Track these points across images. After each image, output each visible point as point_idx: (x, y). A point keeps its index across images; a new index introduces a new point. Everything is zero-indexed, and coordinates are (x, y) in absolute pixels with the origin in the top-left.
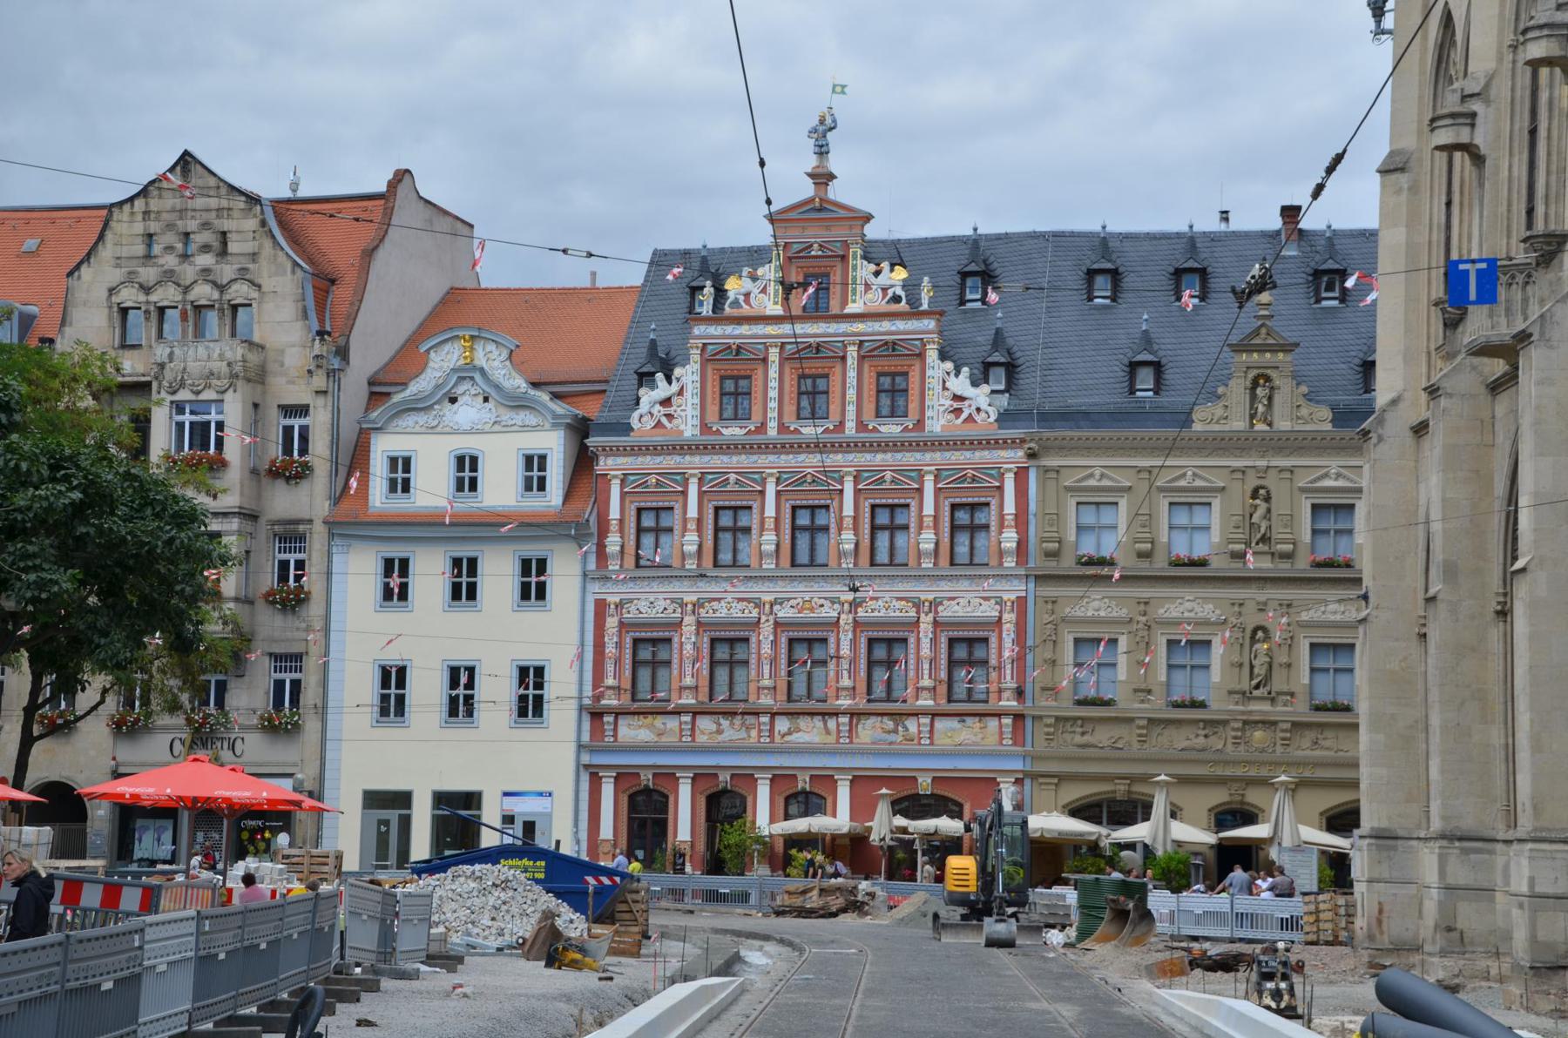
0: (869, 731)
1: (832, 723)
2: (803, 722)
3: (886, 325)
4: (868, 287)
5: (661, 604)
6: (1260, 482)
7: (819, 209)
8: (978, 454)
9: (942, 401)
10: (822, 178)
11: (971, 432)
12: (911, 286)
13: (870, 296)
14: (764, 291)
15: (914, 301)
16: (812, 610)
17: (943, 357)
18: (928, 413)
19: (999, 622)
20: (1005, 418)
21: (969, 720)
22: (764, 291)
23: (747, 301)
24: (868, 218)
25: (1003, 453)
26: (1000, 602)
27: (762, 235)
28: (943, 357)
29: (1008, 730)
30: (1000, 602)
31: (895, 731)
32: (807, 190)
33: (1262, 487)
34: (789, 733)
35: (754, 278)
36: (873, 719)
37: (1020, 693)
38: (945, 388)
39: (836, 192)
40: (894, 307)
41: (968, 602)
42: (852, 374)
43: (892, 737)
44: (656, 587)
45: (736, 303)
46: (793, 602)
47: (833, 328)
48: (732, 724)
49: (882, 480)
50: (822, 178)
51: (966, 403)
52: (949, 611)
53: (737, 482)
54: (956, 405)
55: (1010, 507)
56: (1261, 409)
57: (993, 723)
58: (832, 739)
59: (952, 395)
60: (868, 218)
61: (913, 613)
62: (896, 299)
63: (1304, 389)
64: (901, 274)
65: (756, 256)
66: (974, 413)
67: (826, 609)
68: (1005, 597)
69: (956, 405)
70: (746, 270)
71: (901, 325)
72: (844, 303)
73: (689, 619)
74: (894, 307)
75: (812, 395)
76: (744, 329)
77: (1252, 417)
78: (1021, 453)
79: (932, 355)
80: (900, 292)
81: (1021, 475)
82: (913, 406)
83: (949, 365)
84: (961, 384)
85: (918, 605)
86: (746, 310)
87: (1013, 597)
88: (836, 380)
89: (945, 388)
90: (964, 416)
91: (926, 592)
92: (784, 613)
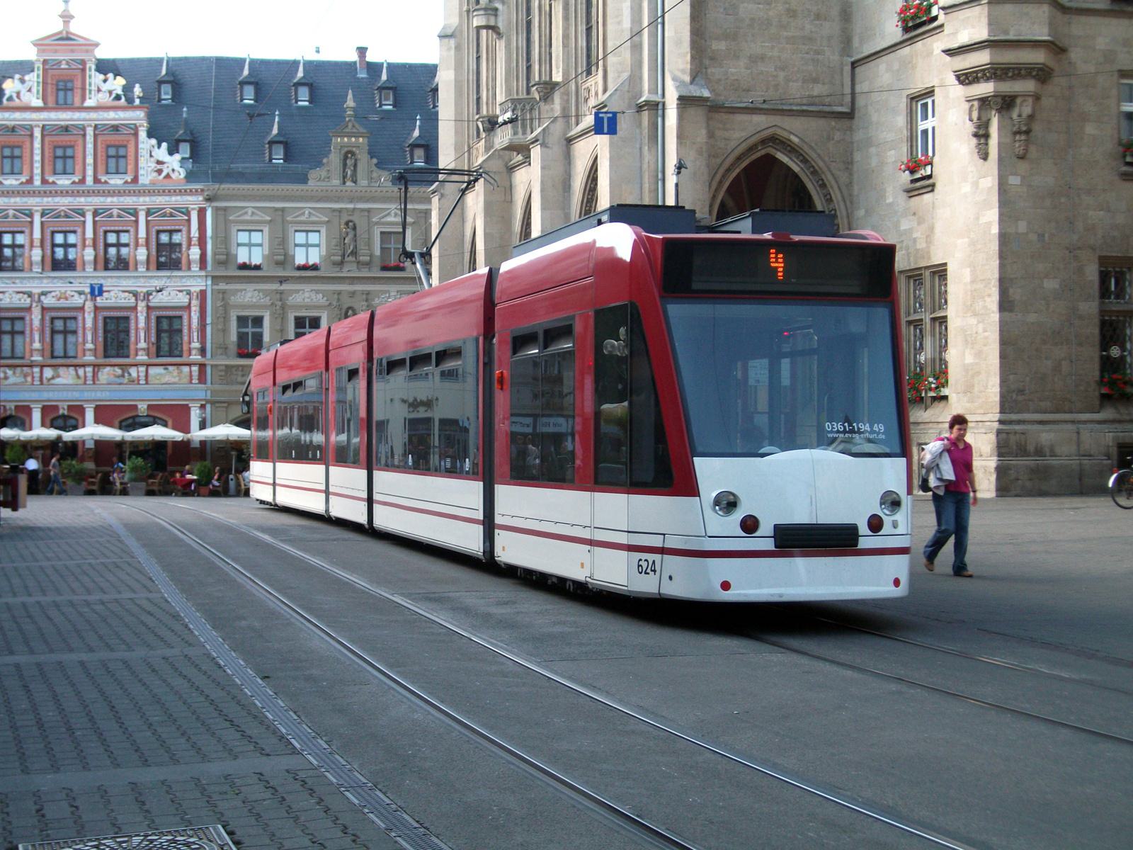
0: (106, 374)
1: (81, 371)
2: (62, 371)
3: (112, 114)
4: (99, 90)
6: (351, 218)
7: (65, 38)
8: (174, 198)
9: (149, 165)
10: (67, 17)
11: (170, 186)
12: (128, 89)
13: (100, 95)
14: (30, 90)
15: (130, 101)
16: (66, 299)
17: (150, 135)
18: (141, 172)
19: (189, 307)
20: (190, 177)
21: (171, 368)
22: (30, 90)
23: (18, 96)
24: (97, 45)
25: (190, 198)
26: (189, 293)
27: (31, 54)
28: (150, 135)
30: (189, 293)
31: (123, 376)
32: (57, 26)
33: (351, 221)
34: (53, 378)
35: (22, 81)
36: (108, 369)
37: (203, 351)
38: (151, 156)
39: (74, 28)
40: (117, 103)
43: (119, 380)
45: (10, 99)
46: (53, 294)
47: (77, 115)
48: (14, 373)
50: (67, 17)
51: (165, 165)
52: (157, 300)
53: (15, 216)
54: (159, 167)
55: (195, 232)
56: (349, 173)
57: (186, 369)
58: (81, 381)
59: (159, 161)
60: (97, 45)
61: (133, 300)
62: (118, 98)
63: (375, 161)
64: (121, 81)
65: (22, 68)
68: (193, 289)
69: (159, 167)
70: (17, 76)
71: (121, 114)
72: (83, 99)
74: (117, 103)
76: (17, 115)
77: (344, 177)
78: (201, 198)
79: (143, 134)
80: (120, 92)
81: (202, 212)
82: (131, 167)
83: (154, 141)
84: (162, 153)
85: (135, 295)
86: (17, 102)
87: (198, 289)
88: (79, 149)
89: (151, 156)
90: (164, 174)
91: (142, 286)
92: (48, 301)
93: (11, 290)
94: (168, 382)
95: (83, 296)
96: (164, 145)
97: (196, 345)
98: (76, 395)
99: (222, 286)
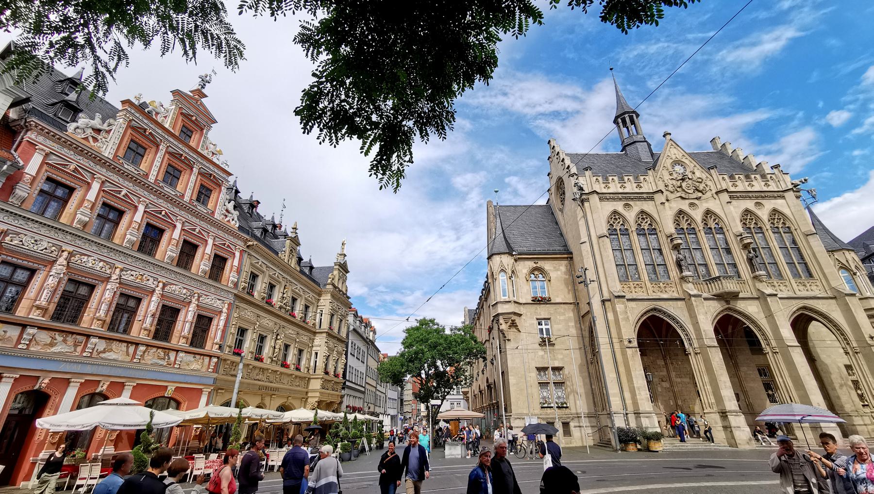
2: (115, 345)
5: (45, 244)
20: (240, 228)
24: (215, 122)
36: (155, 349)
41: (212, 301)
42: (193, 178)
44: (43, 231)
46: (132, 273)
49: (194, 230)
55: (236, 263)
60: (215, 122)
67: (150, 282)
73: (62, 260)
75: (172, 175)
81: (242, 252)
82: (210, 205)
93: (96, 256)
96: (233, 203)
97: (218, 340)
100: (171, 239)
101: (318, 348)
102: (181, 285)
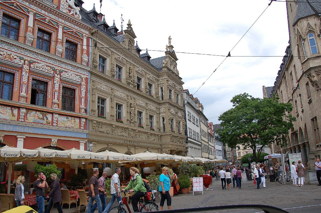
0: (32, 117)
1: (16, 111)
21: (70, 118)
29: (83, 124)
36: (34, 112)
41: (72, 74)
43: (41, 121)
58: (15, 118)
66: (74, 14)
68: (83, 76)
81: (88, 38)
94: (67, 125)
95: (23, 61)
97: (83, 106)
98: (11, 128)
99: (94, 78)
100: (27, 27)
101: (164, 114)
102: (44, 64)
